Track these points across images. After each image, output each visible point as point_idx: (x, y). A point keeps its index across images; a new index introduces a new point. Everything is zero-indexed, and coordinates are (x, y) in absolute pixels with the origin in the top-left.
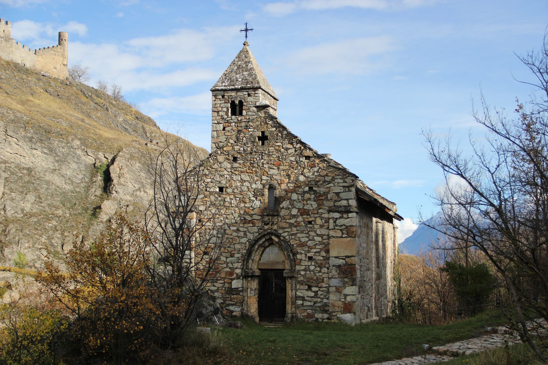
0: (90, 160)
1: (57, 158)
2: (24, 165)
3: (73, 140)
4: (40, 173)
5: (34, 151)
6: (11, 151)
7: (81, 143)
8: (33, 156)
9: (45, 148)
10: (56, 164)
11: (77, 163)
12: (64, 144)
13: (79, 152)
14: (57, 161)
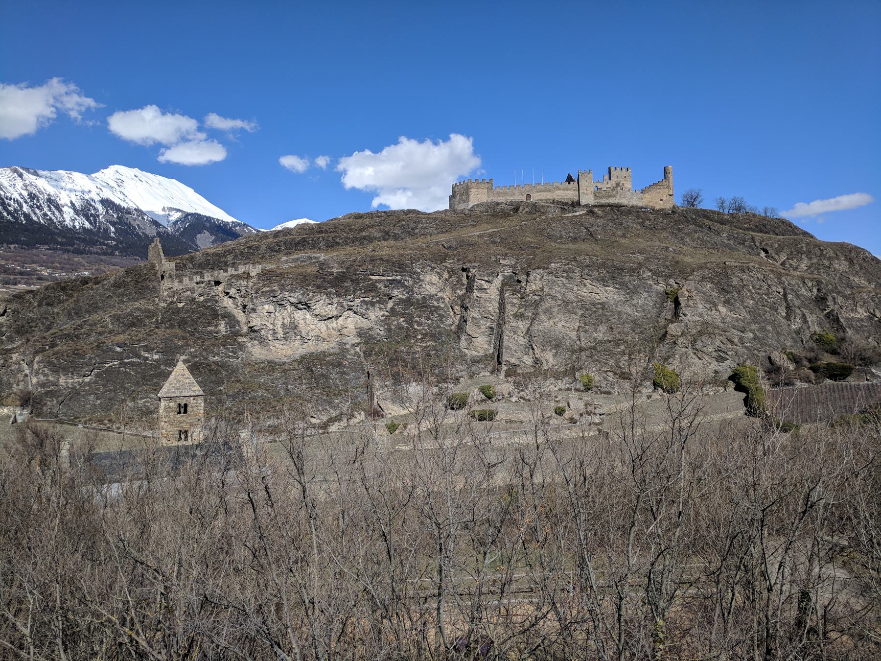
0: (661, 288)
1: (628, 291)
2: (598, 301)
3: (644, 272)
4: (612, 306)
5: (607, 288)
6: (586, 291)
7: (653, 273)
8: (606, 291)
9: (616, 283)
10: (628, 296)
11: (648, 292)
12: (635, 278)
13: (650, 282)
14: (628, 293)
